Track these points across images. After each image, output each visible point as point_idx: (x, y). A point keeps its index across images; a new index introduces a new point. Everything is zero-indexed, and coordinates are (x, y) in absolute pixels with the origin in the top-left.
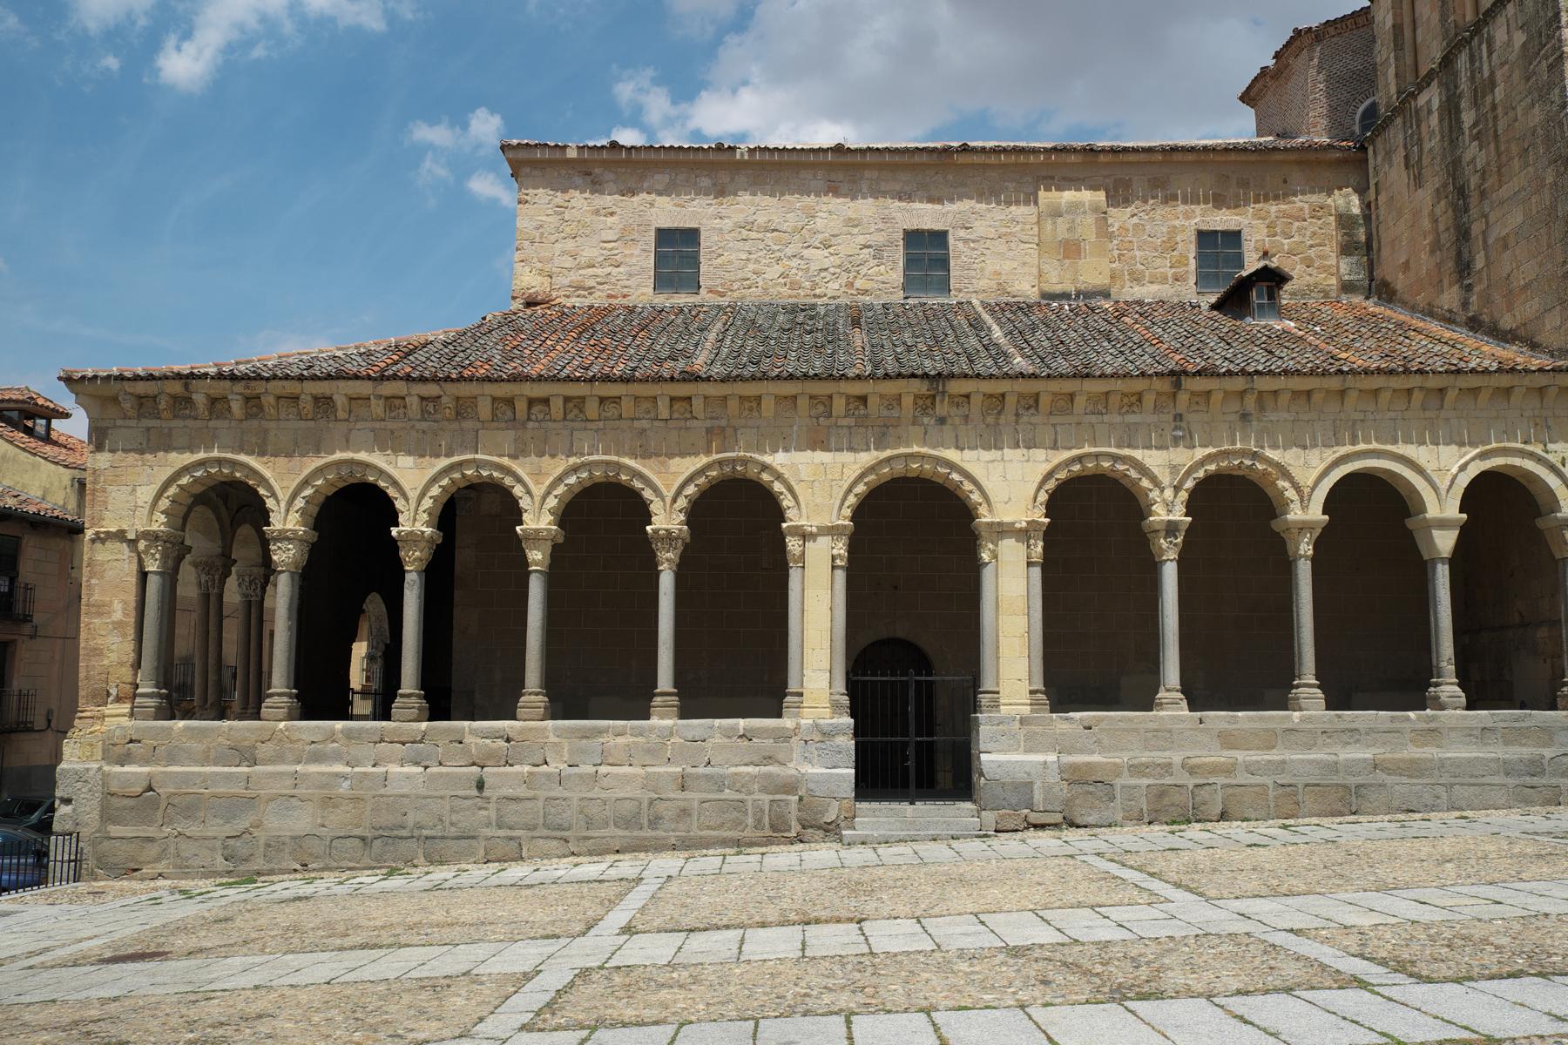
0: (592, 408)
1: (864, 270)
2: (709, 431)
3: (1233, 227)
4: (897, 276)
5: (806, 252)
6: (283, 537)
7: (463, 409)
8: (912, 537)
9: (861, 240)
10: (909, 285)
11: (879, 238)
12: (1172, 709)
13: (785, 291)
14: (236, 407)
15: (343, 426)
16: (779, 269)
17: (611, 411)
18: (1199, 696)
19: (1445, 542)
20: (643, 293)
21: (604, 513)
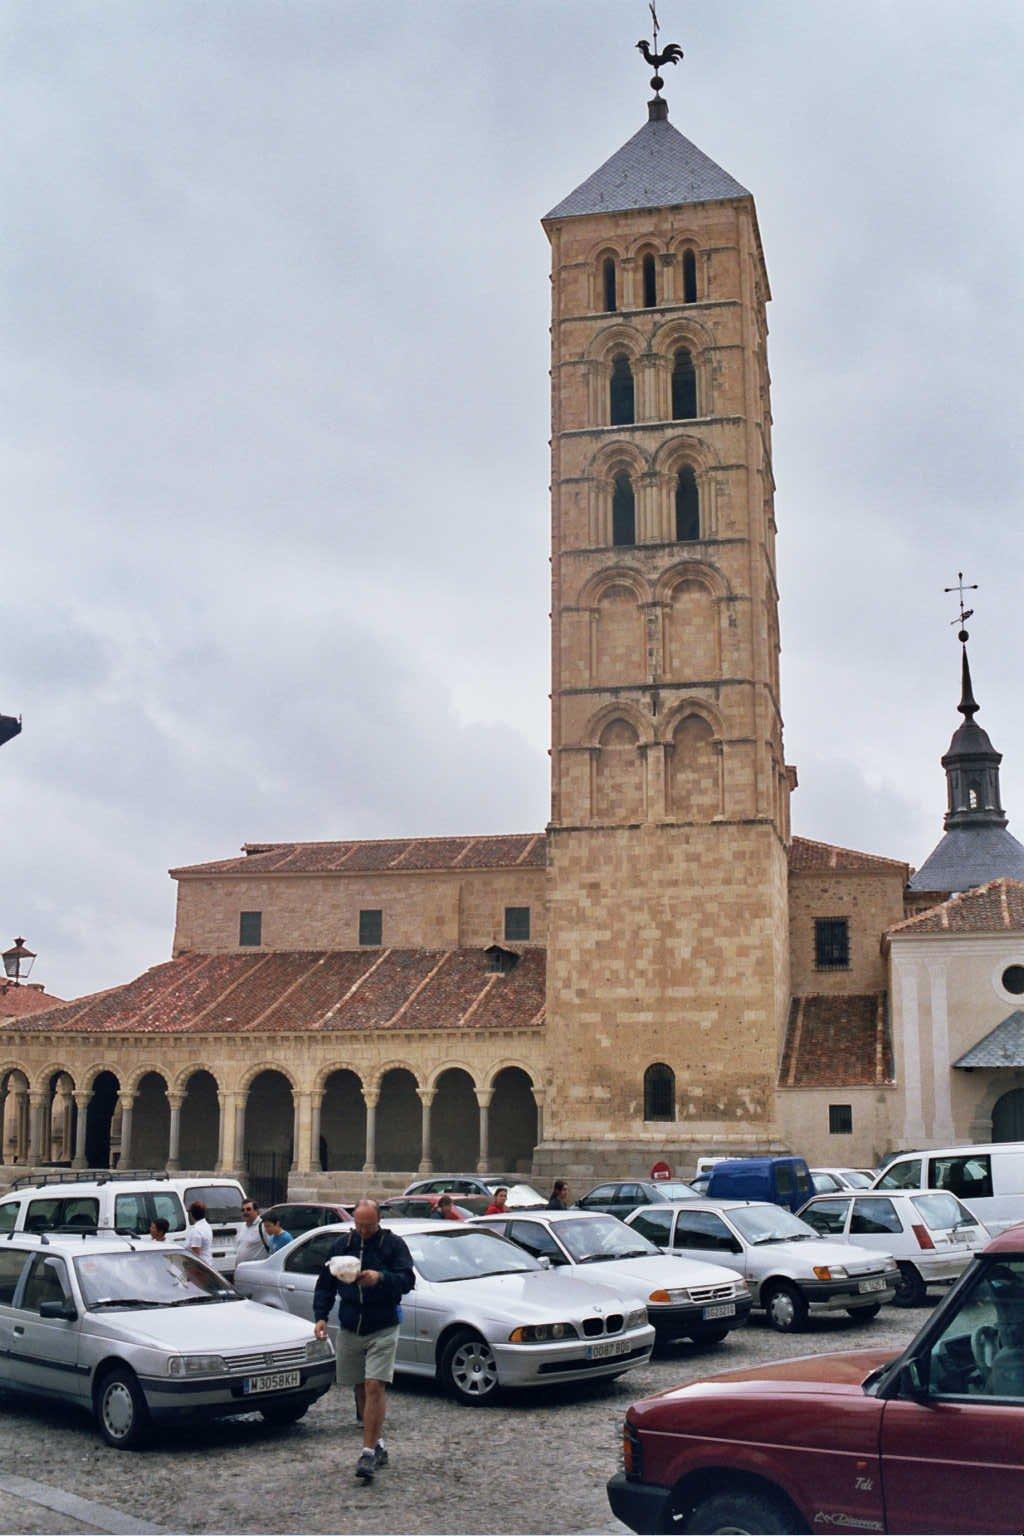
0: (145, 1042)
1: (340, 932)
2: (190, 1052)
3: (524, 906)
5: (314, 924)
6: (35, 1094)
7: (98, 1042)
8: (270, 1094)
9: (340, 916)
10: (362, 941)
11: (348, 915)
12: (368, 1171)
14: (17, 1041)
15: (55, 1050)
17: (152, 1044)
18: (381, 1164)
19: (483, 1100)
20: (235, 947)
21: (152, 1083)
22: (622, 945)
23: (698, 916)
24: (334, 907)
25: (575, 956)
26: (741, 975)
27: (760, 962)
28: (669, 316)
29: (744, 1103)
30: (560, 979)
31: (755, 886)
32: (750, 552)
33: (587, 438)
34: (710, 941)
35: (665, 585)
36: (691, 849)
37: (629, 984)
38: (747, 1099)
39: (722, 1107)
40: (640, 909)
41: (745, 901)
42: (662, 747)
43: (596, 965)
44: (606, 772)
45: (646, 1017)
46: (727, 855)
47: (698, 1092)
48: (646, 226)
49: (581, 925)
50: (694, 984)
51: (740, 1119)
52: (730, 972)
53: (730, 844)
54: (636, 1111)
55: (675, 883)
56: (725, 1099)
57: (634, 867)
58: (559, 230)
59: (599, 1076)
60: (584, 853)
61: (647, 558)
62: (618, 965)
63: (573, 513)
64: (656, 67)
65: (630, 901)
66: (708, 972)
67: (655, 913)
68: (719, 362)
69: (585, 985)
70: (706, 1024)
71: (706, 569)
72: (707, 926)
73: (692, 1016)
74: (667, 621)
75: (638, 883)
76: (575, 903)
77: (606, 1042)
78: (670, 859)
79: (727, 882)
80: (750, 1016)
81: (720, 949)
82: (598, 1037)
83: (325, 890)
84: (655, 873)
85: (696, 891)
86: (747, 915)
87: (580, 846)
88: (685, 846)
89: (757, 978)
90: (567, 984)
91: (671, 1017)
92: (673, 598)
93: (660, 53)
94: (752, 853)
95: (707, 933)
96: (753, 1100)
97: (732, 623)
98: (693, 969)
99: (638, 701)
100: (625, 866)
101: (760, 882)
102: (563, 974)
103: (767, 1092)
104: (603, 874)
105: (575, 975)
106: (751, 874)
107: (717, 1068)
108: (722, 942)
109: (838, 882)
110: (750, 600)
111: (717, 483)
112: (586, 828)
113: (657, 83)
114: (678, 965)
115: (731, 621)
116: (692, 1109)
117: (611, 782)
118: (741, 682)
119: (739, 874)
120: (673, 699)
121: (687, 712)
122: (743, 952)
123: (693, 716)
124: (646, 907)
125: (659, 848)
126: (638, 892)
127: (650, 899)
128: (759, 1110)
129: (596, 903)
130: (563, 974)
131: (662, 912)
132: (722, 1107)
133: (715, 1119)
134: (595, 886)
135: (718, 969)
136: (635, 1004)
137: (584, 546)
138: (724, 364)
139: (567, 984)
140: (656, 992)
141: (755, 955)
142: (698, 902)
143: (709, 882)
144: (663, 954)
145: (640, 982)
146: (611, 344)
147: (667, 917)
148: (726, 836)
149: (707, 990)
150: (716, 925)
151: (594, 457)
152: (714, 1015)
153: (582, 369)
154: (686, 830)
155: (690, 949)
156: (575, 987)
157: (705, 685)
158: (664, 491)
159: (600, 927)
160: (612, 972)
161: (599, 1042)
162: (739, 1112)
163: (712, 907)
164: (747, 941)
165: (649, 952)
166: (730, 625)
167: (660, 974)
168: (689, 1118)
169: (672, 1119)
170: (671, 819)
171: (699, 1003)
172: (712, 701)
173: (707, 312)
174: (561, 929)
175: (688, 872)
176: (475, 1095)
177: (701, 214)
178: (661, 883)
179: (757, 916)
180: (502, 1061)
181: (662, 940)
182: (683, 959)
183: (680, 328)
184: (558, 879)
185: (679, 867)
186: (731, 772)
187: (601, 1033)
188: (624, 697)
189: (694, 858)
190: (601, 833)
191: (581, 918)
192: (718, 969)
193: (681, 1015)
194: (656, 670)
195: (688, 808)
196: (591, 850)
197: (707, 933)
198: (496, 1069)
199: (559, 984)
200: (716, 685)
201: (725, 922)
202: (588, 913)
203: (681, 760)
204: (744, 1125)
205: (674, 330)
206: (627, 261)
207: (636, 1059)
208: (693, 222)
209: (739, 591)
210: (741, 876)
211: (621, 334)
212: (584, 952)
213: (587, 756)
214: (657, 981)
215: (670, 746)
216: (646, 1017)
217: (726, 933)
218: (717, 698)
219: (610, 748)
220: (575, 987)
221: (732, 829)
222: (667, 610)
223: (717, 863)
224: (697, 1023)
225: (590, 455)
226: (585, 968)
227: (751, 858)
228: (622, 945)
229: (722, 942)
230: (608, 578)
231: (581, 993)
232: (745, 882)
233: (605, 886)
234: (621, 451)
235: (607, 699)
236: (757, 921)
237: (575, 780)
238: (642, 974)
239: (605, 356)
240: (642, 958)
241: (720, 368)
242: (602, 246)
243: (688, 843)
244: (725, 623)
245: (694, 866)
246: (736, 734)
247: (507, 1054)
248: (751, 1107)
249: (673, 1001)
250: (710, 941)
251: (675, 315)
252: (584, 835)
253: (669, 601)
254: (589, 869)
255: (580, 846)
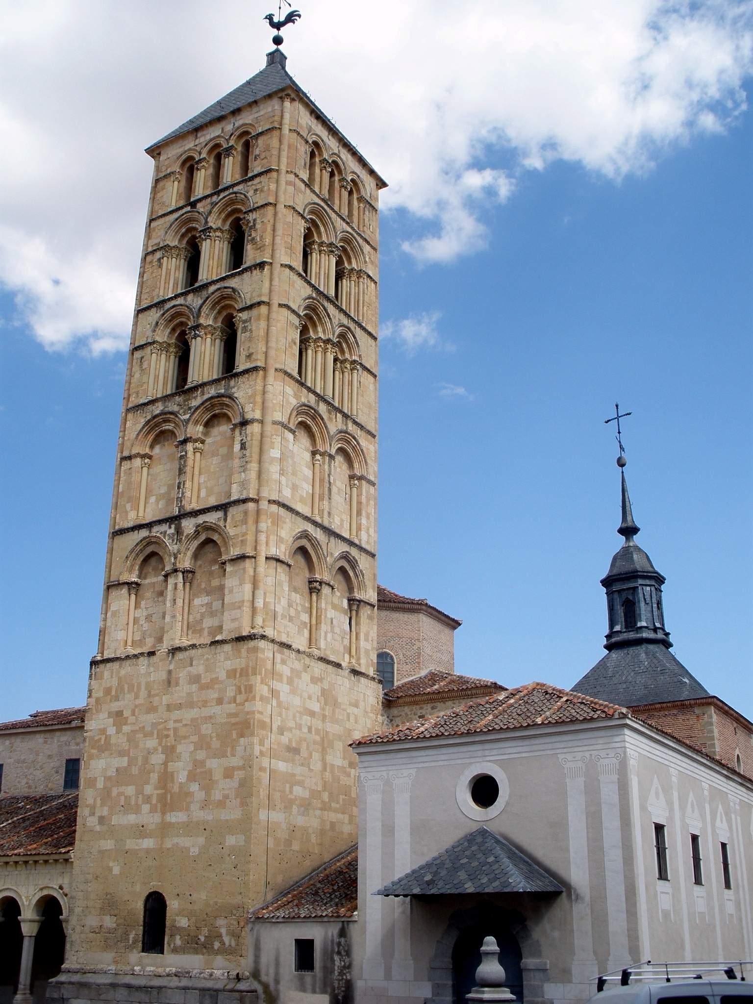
4: (62, 782)
11: (57, 764)
13: (26, 790)
16: (25, 781)
22: (135, 770)
23: (195, 738)
24: (50, 757)
25: (100, 784)
26: (226, 797)
27: (243, 783)
28: (222, 195)
29: (221, 936)
30: (87, 806)
31: (242, 704)
32: (265, 377)
33: (154, 310)
34: (202, 763)
35: (196, 422)
36: (193, 670)
37: (137, 810)
38: (223, 931)
39: (202, 939)
40: (151, 734)
41: (233, 720)
42: (180, 575)
43: (115, 792)
44: (143, 603)
45: (148, 843)
46: (222, 675)
47: (183, 922)
48: (214, 132)
49: (107, 753)
50: (188, 809)
51: (218, 952)
52: (217, 795)
53: (226, 660)
54: (135, 942)
55: (179, 707)
56: (205, 931)
57: (149, 695)
58: (159, 154)
59: (110, 905)
60: (115, 682)
61: (185, 401)
62: (130, 790)
63: (137, 375)
64: (279, 29)
65: (144, 727)
66: (199, 795)
67: (162, 737)
68: (255, 220)
69: (105, 812)
70: (194, 851)
71: (226, 400)
72: (202, 748)
73: (184, 842)
74: (198, 454)
75: (152, 709)
76: (103, 731)
77: (116, 870)
78: (177, 684)
79: (220, 702)
80: (231, 840)
81: (210, 771)
82: (111, 864)
83: (46, 742)
84: (164, 698)
85: (193, 713)
86: (234, 736)
87: (112, 677)
88: (189, 668)
89: (238, 800)
90: (93, 814)
91: (168, 844)
92: (206, 434)
93: (282, 19)
94: (242, 669)
95: (201, 755)
96: (228, 933)
97: (243, 446)
98: (189, 794)
99: (165, 532)
100: (143, 693)
101: (246, 700)
102: (90, 801)
103: (242, 924)
104: (125, 704)
105: (99, 802)
106: (240, 693)
107: (201, 896)
108: (213, 764)
109: (433, 708)
110: (262, 422)
111: (245, 322)
112: (117, 658)
113: (278, 41)
114: (176, 789)
115: (242, 444)
116: (178, 941)
117: (145, 614)
118: (244, 501)
119: (230, 692)
120: (191, 526)
121: (203, 537)
122: (228, 773)
123: (209, 541)
124: (155, 732)
125: (170, 672)
126: (151, 718)
127: (159, 723)
128: (233, 944)
129: (118, 731)
130: (90, 801)
131: (167, 736)
132: (202, 939)
133: (196, 952)
134: (119, 714)
135: (208, 794)
136: (141, 831)
137: (142, 401)
138: (258, 221)
139: (93, 814)
140: (157, 818)
141: (239, 775)
142: (195, 724)
143: (205, 704)
144: (166, 777)
145: (146, 808)
146: (184, 230)
147: (170, 741)
148: (222, 657)
149: (198, 814)
150: (209, 747)
151: (157, 323)
152: (201, 840)
153: (158, 255)
154: (193, 652)
155: (186, 773)
156: (98, 814)
157: (216, 508)
158: (209, 340)
159: (121, 754)
160: (126, 797)
161: (110, 869)
162: (217, 945)
163: (206, 729)
164: (235, 761)
165: (154, 777)
166: (241, 448)
167: (162, 798)
168: (175, 950)
169: (162, 953)
170: (177, 643)
171: (190, 828)
172: (221, 524)
173: (250, 183)
174: (91, 757)
175: (189, 694)
176: (19, 923)
177: (255, 109)
178: (169, 708)
179: (242, 735)
180: (42, 889)
181: (165, 764)
182: (181, 783)
183: (232, 202)
184: (94, 711)
185: (183, 690)
186: (231, 591)
187: (114, 861)
188: (155, 529)
189: (195, 679)
190: (128, 662)
191: (105, 747)
192: (208, 794)
193: (176, 840)
194: (181, 501)
195: (201, 631)
196: (120, 679)
197: (201, 755)
198: (37, 897)
199: (86, 812)
200: (223, 507)
201: (216, 744)
202: (113, 741)
203: (199, 585)
204: (219, 960)
205: (227, 205)
206: (200, 161)
207: (138, 888)
208: (246, 118)
209: (249, 416)
210: (232, 694)
211: (190, 220)
212: (108, 779)
213: (125, 591)
214: (159, 805)
215: (188, 572)
216: (148, 843)
217: (215, 756)
218: (225, 520)
219: (147, 581)
220: (98, 814)
221: (227, 648)
222: (197, 445)
223: (215, 681)
224: (188, 849)
225: (154, 323)
226: (106, 794)
227: (241, 675)
228: (135, 770)
229: (213, 764)
230: (157, 425)
231: (102, 820)
232: (235, 702)
233: (126, 714)
234: (179, 314)
235: (144, 533)
236: (242, 740)
237: (114, 614)
238: (148, 799)
239: (180, 241)
240: (148, 783)
241: (254, 225)
242: (184, 157)
243: (191, 665)
244: (237, 447)
245: (194, 687)
246: (235, 552)
247: (43, 882)
248: (226, 939)
249: (171, 825)
250: (202, 763)
251: (227, 193)
252: (115, 665)
253: (200, 435)
254: (117, 699)
255: (112, 677)
